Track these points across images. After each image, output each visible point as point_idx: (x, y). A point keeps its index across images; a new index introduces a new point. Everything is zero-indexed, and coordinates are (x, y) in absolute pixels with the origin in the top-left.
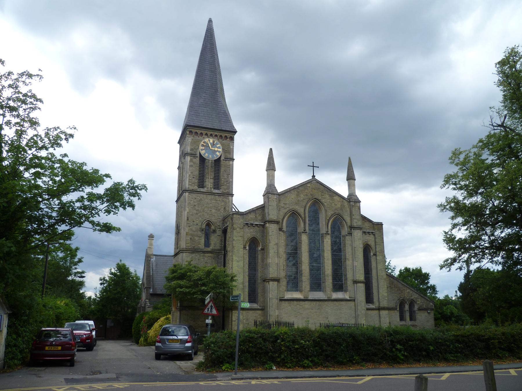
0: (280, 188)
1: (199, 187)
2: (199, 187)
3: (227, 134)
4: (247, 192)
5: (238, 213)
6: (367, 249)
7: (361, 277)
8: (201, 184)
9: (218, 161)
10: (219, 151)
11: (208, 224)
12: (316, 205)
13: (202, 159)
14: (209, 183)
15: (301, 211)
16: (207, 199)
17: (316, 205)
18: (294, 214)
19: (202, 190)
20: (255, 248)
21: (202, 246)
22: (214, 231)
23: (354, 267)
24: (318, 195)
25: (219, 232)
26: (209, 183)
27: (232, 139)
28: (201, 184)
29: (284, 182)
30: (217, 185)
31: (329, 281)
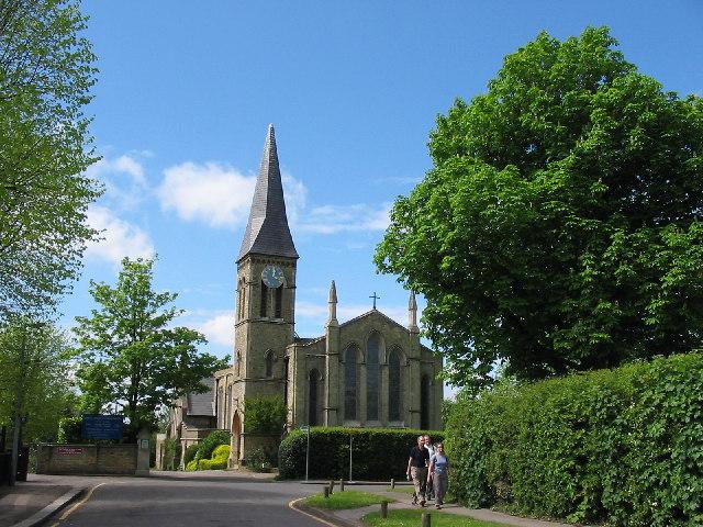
0: (341, 320)
1: (262, 316)
2: (262, 316)
3: (290, 262)
4: (310, 319)
5: (297, 340)
6: (425, 380)
7: (417, 406)
8: (263, 314)
9: (279, 290)
10: (282, 280)
11: (270, 354)
12: (375, 336)
13: (264, 288)
14: (271, 312)
15: (361, 342)
16: (270, 329)
17: (375, 336)
18: (353, 347)
19: (264, 319)
20: (313, 380)
21: (264, 374)
22: (276, 361)
23: (411, 397)
24: (377, 324)
25: (281, 362)
26: (271, 312)
27: (294, 265)
28: (263, 314)
29: (346, 314)
30: (278, 315)
31: (385, 411)
